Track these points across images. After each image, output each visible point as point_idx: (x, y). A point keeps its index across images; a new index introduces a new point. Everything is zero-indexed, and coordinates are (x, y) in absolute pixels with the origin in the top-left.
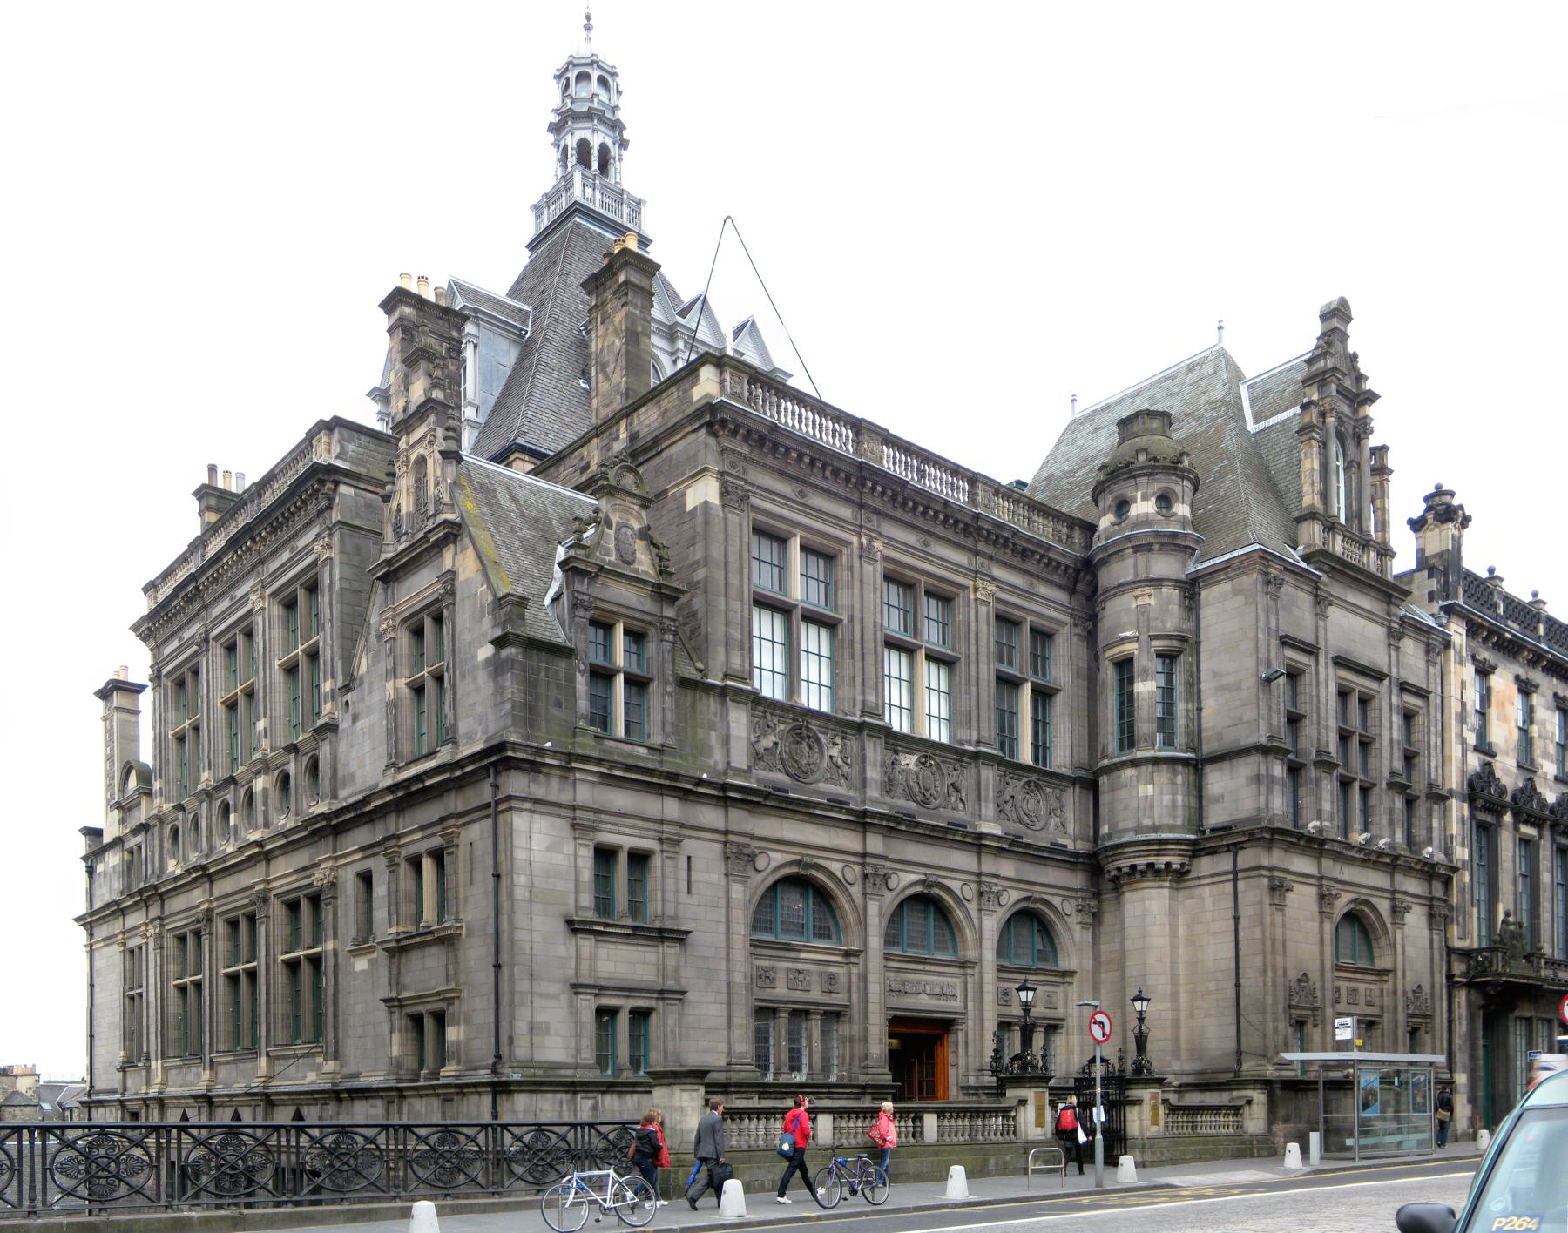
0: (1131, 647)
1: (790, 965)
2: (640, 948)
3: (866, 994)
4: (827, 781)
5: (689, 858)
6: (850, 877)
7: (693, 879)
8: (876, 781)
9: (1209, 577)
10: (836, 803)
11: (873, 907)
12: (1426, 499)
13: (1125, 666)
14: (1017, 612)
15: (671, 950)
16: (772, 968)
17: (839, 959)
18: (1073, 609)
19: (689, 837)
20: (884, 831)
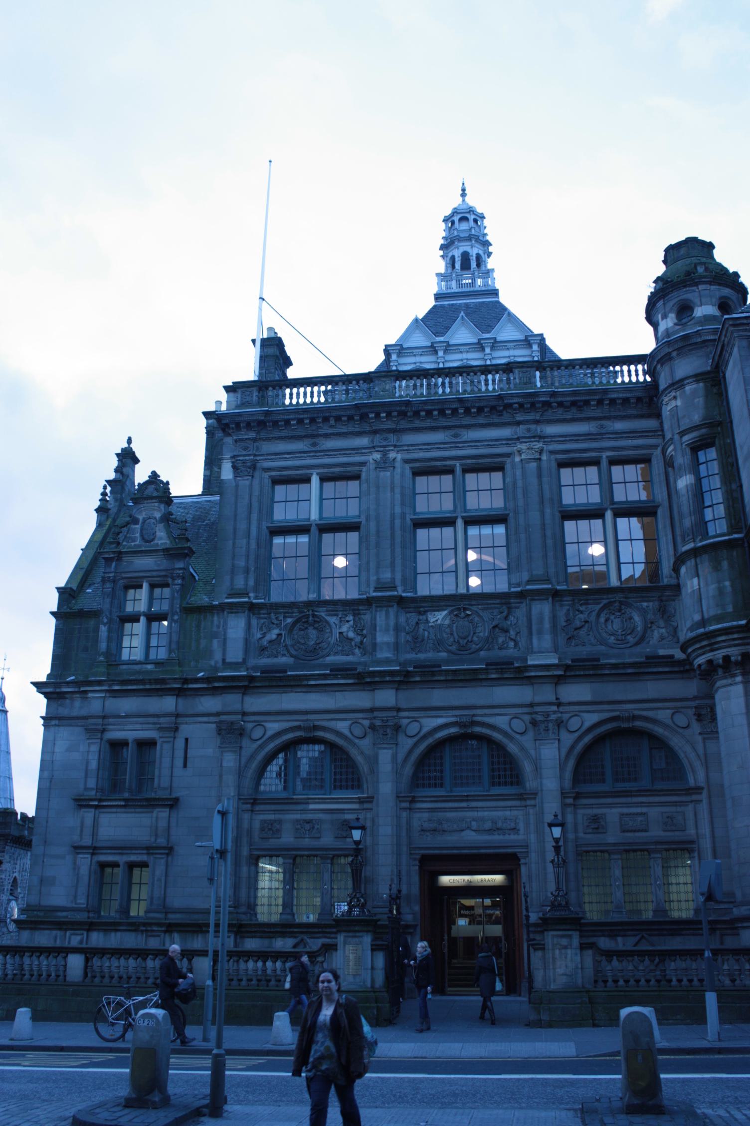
2: (137, 815)
4: (336, 653)
5: (187, 740)
7: (188, 756)
8: (388, 644)
10: (338, 671)
11: (385, 756)
14: (585, 455)
15: (164, 813)
16: (280, 822)
19: (186, 723)
20: (396, 685)
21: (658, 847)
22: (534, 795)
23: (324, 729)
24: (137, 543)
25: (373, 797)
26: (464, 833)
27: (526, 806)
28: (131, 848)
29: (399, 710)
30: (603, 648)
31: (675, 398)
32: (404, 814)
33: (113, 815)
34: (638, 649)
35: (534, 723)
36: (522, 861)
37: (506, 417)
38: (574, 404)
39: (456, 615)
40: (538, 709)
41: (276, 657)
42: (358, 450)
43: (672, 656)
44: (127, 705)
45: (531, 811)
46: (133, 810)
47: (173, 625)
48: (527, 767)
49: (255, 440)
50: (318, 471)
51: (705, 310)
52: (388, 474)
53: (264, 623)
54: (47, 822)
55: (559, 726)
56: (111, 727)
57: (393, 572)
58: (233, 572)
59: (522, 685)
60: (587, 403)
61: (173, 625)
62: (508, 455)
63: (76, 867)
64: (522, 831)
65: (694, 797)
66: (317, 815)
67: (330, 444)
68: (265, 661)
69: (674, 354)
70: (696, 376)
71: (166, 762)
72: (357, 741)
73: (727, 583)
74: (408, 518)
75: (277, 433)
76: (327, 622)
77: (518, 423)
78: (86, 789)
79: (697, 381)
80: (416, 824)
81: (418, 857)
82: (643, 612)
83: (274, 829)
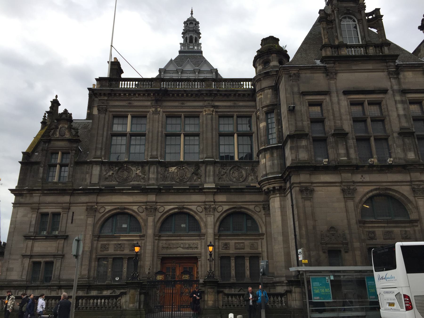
1: (116, 242)
2: (50, 242)
4: (134, 181)
5: (73, 213)
8: (154, 178)
10: (134, 188)
11: (150, 219)
15: (62, 241)
16: (109, 244)
17: (138, 238)
21: (248, 255)
22: (204, 235)
23: (128, 209)
24: (58, 136)
25: (145, 235)
26: (178, 249)
27: (201, 239)
28: (47, 256)
29: (156, 202)
30: (231, 182)
31: (261, 95)
32: (156, 241)
33: (41, 242)
34: (243, 183)
35: (205, 208)
36: (199, 259)
38: (225, 95)
39: (179, 169)
40: (207, 203)
41: (111, 182)
42: (146, 107)
43: (255, 186)
44: (49, 199)
45: (203, 241)
46: (49, 240)
47: (71, 168)
48: (202, 225)
49: (107, 100)
50: (131, 113)
51: (274, 63)
52: (157, 116)
53: (107, 169)
54: (12, 245)
55: (214, 210)
56: (42, 207)
57: (157, 152)
58: (96, 149)
59: (202, 194)
60: (230, 95)
61: (71, 168)
62: (201, 112)
63: (22, 263)
64: (199, 249)
65: (261, 237)
66: (124, 242)
67: (136, 103)
68: (107, 183)
69: (262, 79)
70: (269, 87)
71: (64, 221)
72: (140, 214)
73: (276, 162)
74: (164, 132)
76: (131, 169)
77: (205, 101)
78: (29, 232)
79: (269, 89)
80: (160, 245)
81: (161, 258)
82: (246, 170)
83: (106, 247)
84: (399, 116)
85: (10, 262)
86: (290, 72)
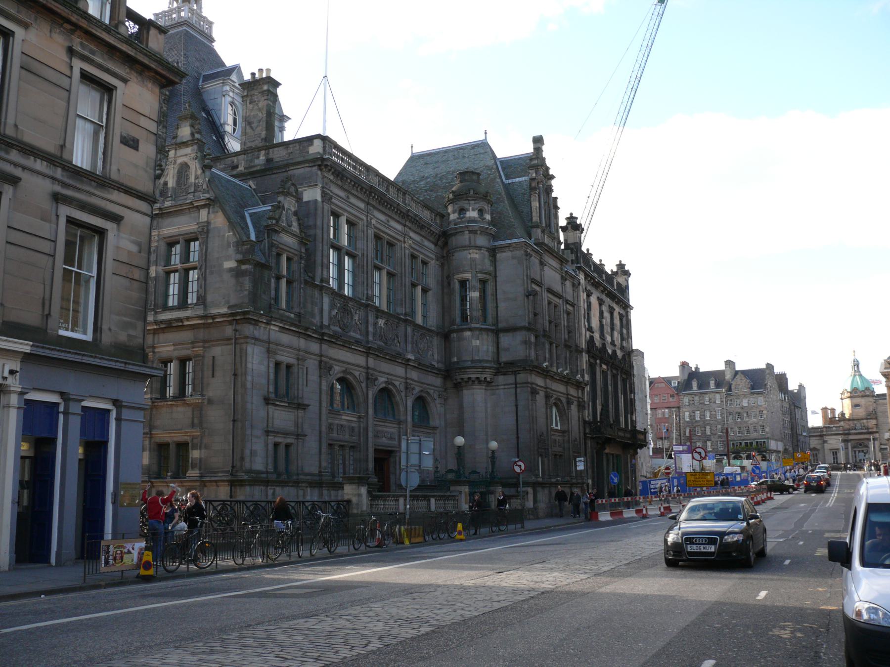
0: (468, 276)
3: (367, 438)
5: (307, 368)
6: (362, 379)
9: (502, 248)
10: (358, 342)
12: (567, 219)
13: (463, 283)
15: (301, 413)
17: (355, 419)
18: (436, 253)
20: (374, 356)
31: (477, 253)
37: (403, 221)
44: (285, 338)
48: (402, 409)
50: (348, 215)
62: (400, 241)
67: (353, 200)
69: (479, 232)
70: (487, 248)
75: (339, 183)
76: (351, 311)
77: (405, 226)
84: (564, 326)
85: (254, 440)
86: (527, 250)
